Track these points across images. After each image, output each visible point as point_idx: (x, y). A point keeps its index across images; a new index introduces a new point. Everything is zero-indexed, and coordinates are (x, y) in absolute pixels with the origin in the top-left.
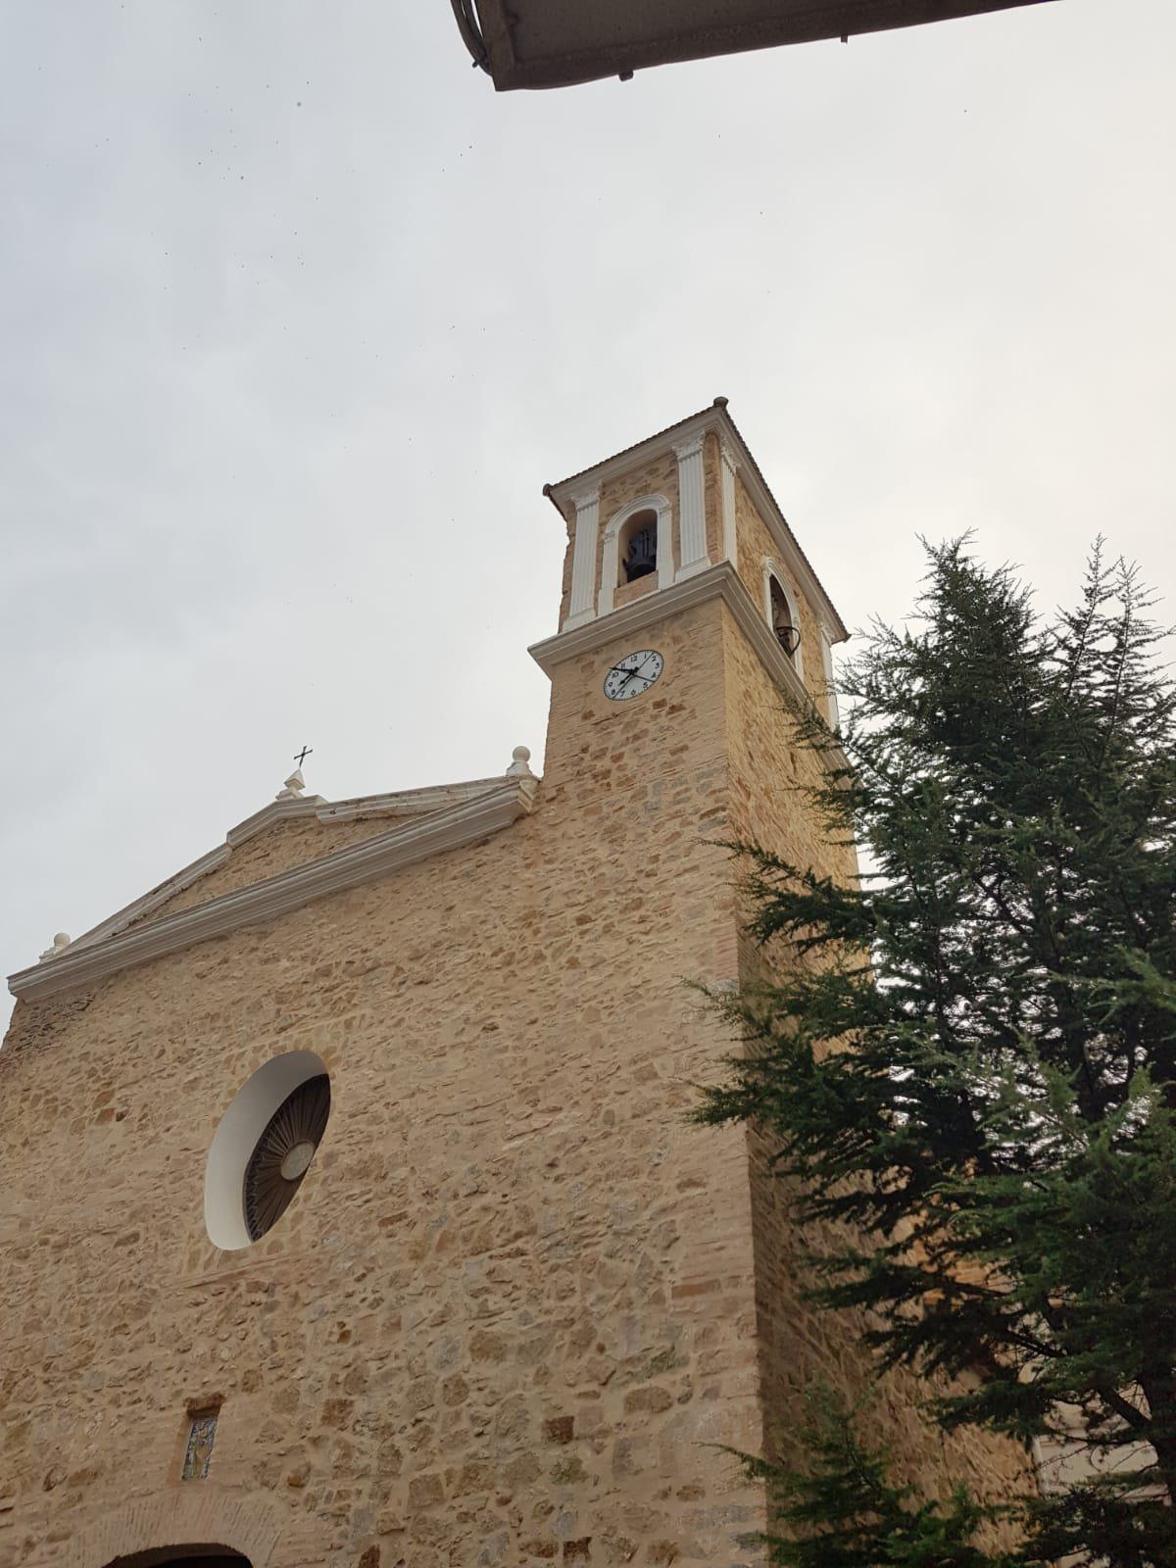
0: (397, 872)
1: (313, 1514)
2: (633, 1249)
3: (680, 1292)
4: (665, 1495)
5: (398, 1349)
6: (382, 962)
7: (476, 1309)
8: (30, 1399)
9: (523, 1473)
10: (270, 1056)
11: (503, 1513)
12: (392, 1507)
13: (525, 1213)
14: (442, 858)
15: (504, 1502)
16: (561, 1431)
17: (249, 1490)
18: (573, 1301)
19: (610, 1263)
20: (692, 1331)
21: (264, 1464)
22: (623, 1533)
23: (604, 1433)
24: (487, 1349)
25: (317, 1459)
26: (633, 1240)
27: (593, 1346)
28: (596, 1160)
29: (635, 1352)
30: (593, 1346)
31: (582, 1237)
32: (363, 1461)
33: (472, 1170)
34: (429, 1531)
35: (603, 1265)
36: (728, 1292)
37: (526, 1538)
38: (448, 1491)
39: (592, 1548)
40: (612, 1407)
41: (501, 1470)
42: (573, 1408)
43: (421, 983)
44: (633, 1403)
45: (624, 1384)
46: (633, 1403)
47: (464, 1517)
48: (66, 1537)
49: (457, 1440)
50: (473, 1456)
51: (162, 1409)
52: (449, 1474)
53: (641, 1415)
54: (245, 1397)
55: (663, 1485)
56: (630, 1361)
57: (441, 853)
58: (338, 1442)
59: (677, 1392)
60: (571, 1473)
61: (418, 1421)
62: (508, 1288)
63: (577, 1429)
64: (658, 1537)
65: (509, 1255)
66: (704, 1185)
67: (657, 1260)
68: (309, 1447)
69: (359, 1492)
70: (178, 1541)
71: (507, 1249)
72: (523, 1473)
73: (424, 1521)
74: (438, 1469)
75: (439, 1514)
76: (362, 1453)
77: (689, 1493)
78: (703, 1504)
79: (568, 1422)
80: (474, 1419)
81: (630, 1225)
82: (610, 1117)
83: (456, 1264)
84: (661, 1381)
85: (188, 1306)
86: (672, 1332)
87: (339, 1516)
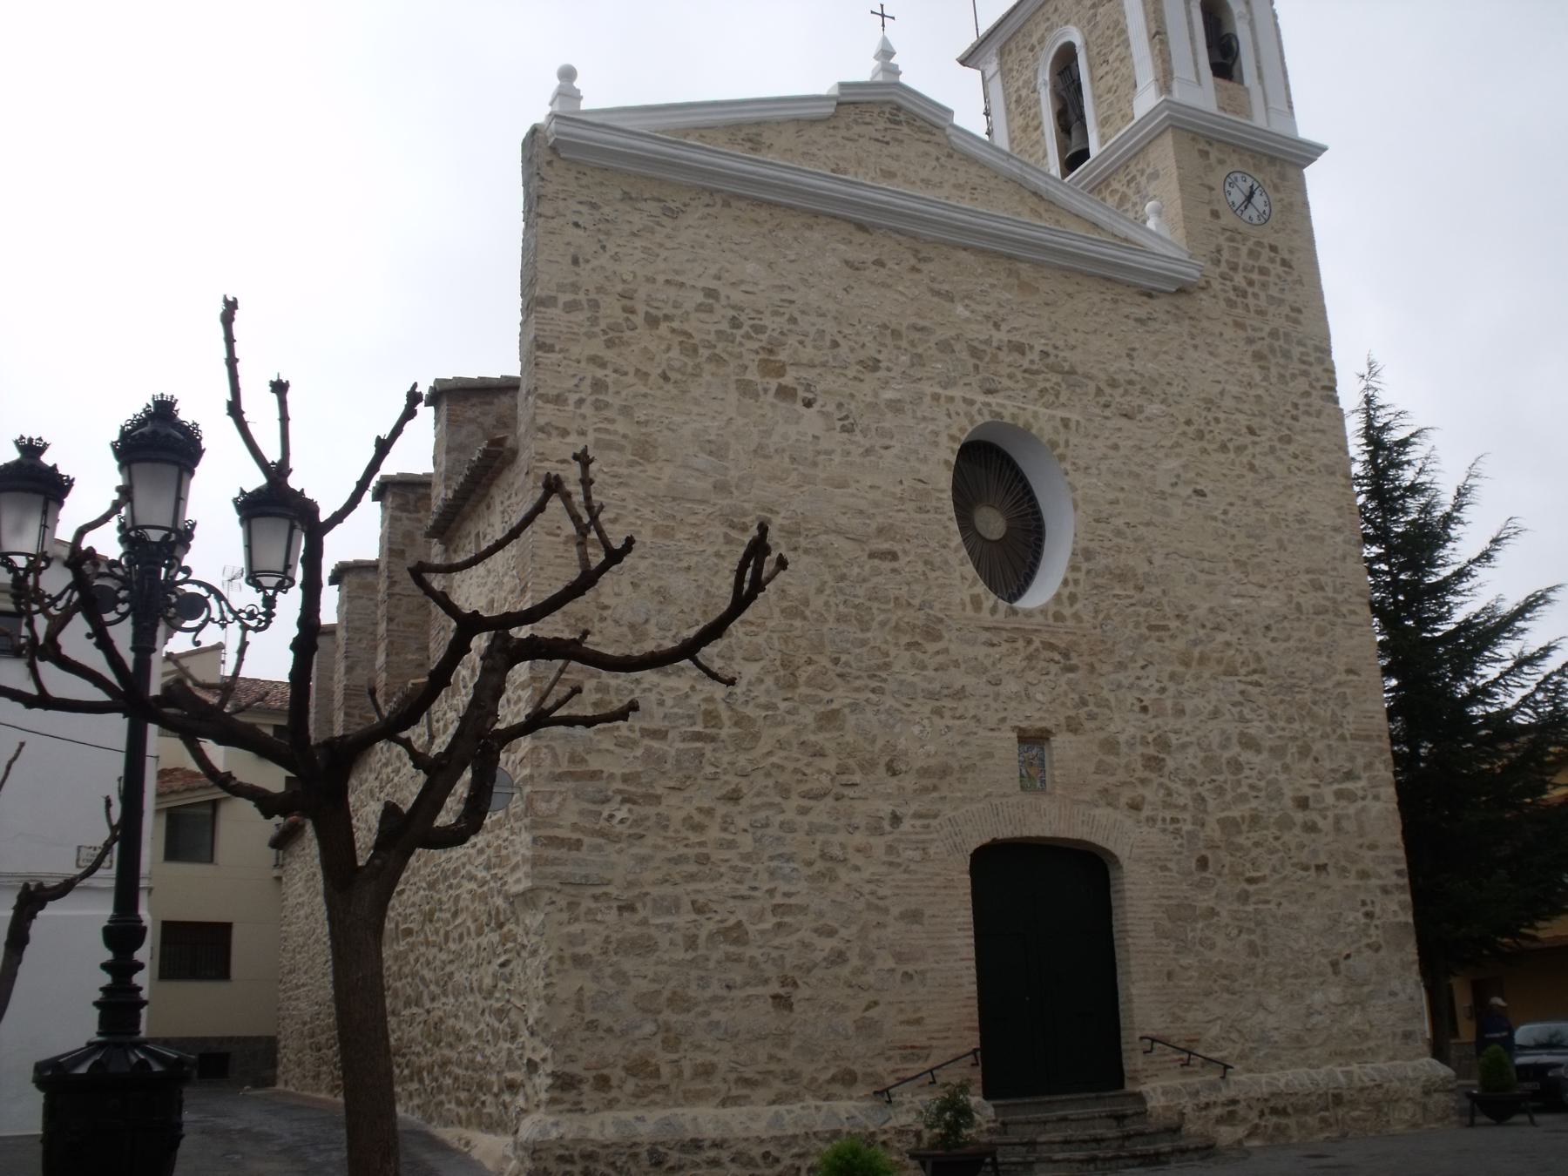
0: (1067, 272)
1: (1154, 830)
2: (1325, 702)
3: (1354, 737)
4: (1361, 846)
5: (1188, 728)
6: (1080, 370)
7: (1237, 716)
8: (828, 688)
9: (1285, 823)
10: (988, 418)
11: (1277, 844)
12: (1208, 830)
13: (1258, 659)
14: (1108, 285)
15: (1277, 838)
16: (1303, 803)
17: (1097, 806)
18: (1296, 726)
19: (1315, 708)
20: (1360, 761)
21: (1106, 790)
22: (1343, 863)
23: (1326, 809)
24: (1249, 743)
25: (1148, 793)
26: (1324, 697)
27: (1311, 758)
28: (1296, 635)
29: (1334, 766)
30: (1311, 758)
31: (1294, 685)
32: (1181, 801)
33: (1211, 610)
34: (1237, 850)
35: (1310, 709)
36: (1377, 744)
37: (1295, 860)
38: (1244, 827)
39: (1330, 869)
40: (1328, 792)
41: (1272, 820)
42: (1309, 792)
43: (1125, 415)
44: (1339, 795)
45: (1331, 783)
46: (1339, 795)
47: (1256, 844)
48: (935, 816)
49: (1242, 798)
50: (1256, 809)
51: (992, 730)
52: (1243, 818)
53: (1343, 803)
54: (1070, 736)
55: (1360, 841)
56: (1333, 770)
57: (1108, 279)
58: (1161, 785)
59: (1360, 793)
60: (1311, 828)
61: (1214, 781)
62: (1254, 706)
63: (1311, 803)
64: (1360, 866)
65: (1250, 683)
66: (1359, 675)
67: (1339, 714)
68: (1138, 784)
69: (1185, 820)
70: (1048, 834)
71: (1249, 679)
72: (1285, 823)
73: (1232, 843)
74: (1235, 813)
75: (1241, 840)
76: (1180, 795)
77: (1372, 847)
78: (1380, 853)
79: (1306, 799)
80: (1252, 787)
81: (1322, 687)
82: (1299, 607)
83: (1215, 679)
84: (1349, 785)
85: (984, 643)
86: (1352, 759)
87: (1177, 832)
